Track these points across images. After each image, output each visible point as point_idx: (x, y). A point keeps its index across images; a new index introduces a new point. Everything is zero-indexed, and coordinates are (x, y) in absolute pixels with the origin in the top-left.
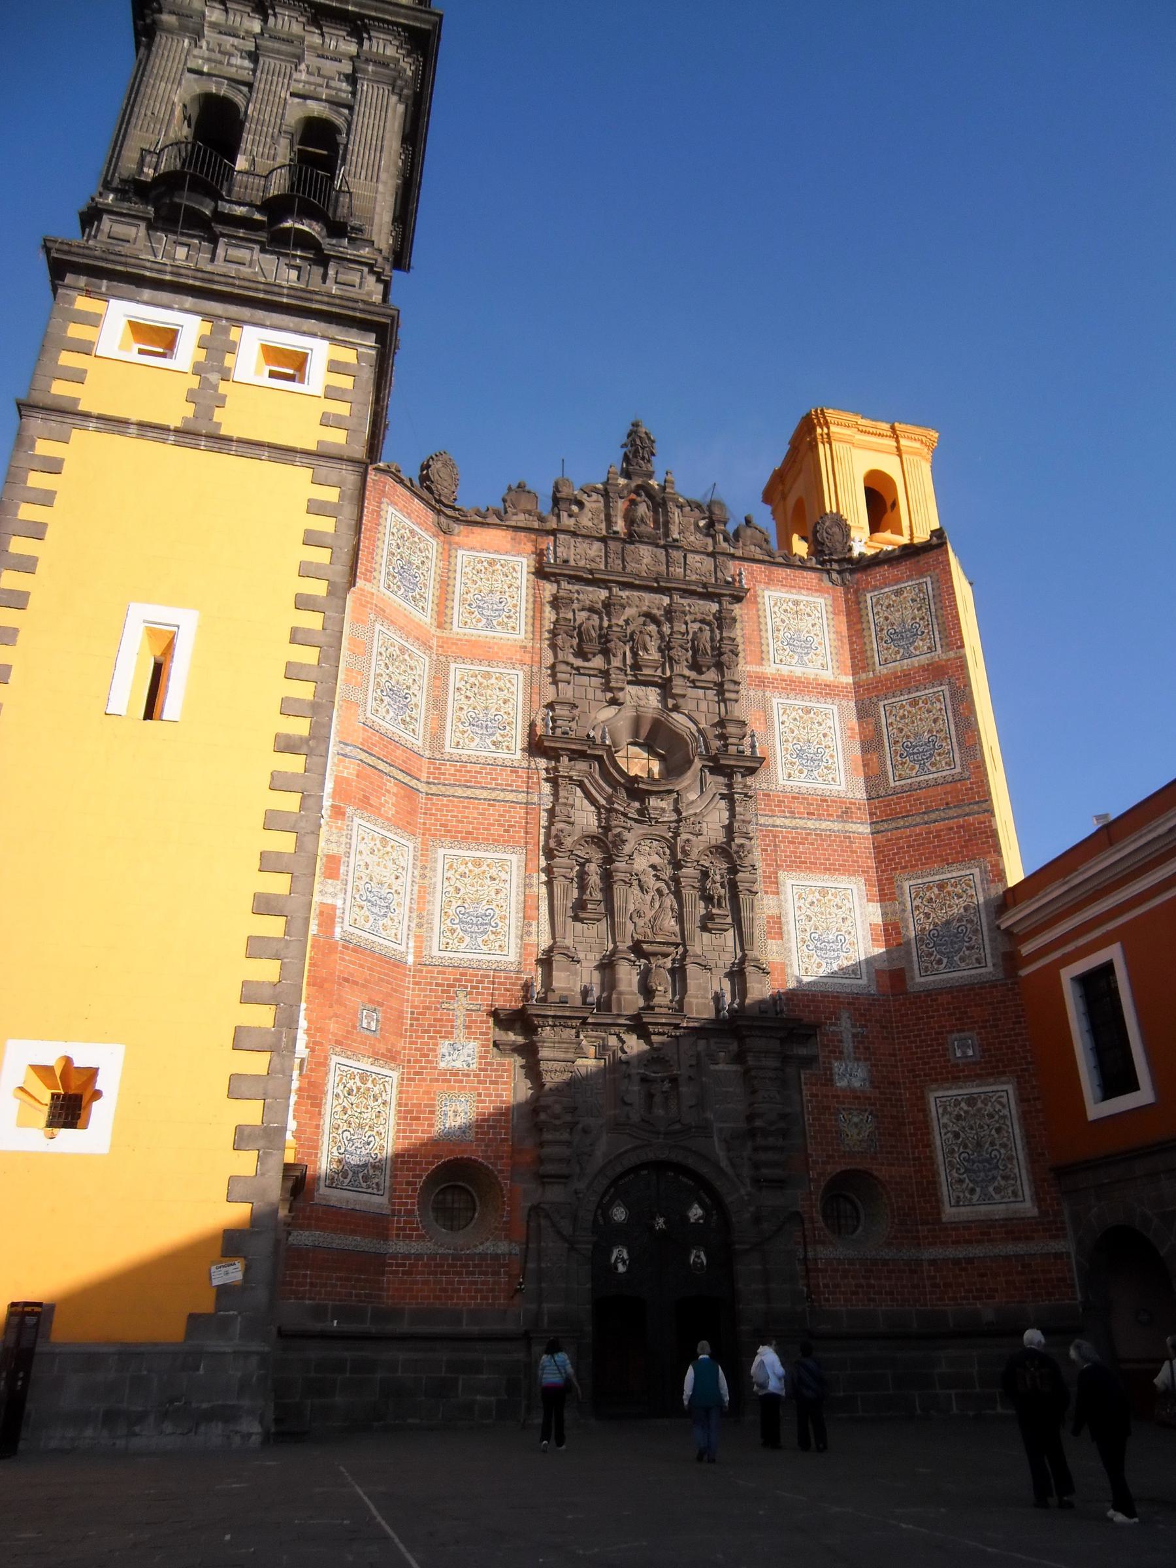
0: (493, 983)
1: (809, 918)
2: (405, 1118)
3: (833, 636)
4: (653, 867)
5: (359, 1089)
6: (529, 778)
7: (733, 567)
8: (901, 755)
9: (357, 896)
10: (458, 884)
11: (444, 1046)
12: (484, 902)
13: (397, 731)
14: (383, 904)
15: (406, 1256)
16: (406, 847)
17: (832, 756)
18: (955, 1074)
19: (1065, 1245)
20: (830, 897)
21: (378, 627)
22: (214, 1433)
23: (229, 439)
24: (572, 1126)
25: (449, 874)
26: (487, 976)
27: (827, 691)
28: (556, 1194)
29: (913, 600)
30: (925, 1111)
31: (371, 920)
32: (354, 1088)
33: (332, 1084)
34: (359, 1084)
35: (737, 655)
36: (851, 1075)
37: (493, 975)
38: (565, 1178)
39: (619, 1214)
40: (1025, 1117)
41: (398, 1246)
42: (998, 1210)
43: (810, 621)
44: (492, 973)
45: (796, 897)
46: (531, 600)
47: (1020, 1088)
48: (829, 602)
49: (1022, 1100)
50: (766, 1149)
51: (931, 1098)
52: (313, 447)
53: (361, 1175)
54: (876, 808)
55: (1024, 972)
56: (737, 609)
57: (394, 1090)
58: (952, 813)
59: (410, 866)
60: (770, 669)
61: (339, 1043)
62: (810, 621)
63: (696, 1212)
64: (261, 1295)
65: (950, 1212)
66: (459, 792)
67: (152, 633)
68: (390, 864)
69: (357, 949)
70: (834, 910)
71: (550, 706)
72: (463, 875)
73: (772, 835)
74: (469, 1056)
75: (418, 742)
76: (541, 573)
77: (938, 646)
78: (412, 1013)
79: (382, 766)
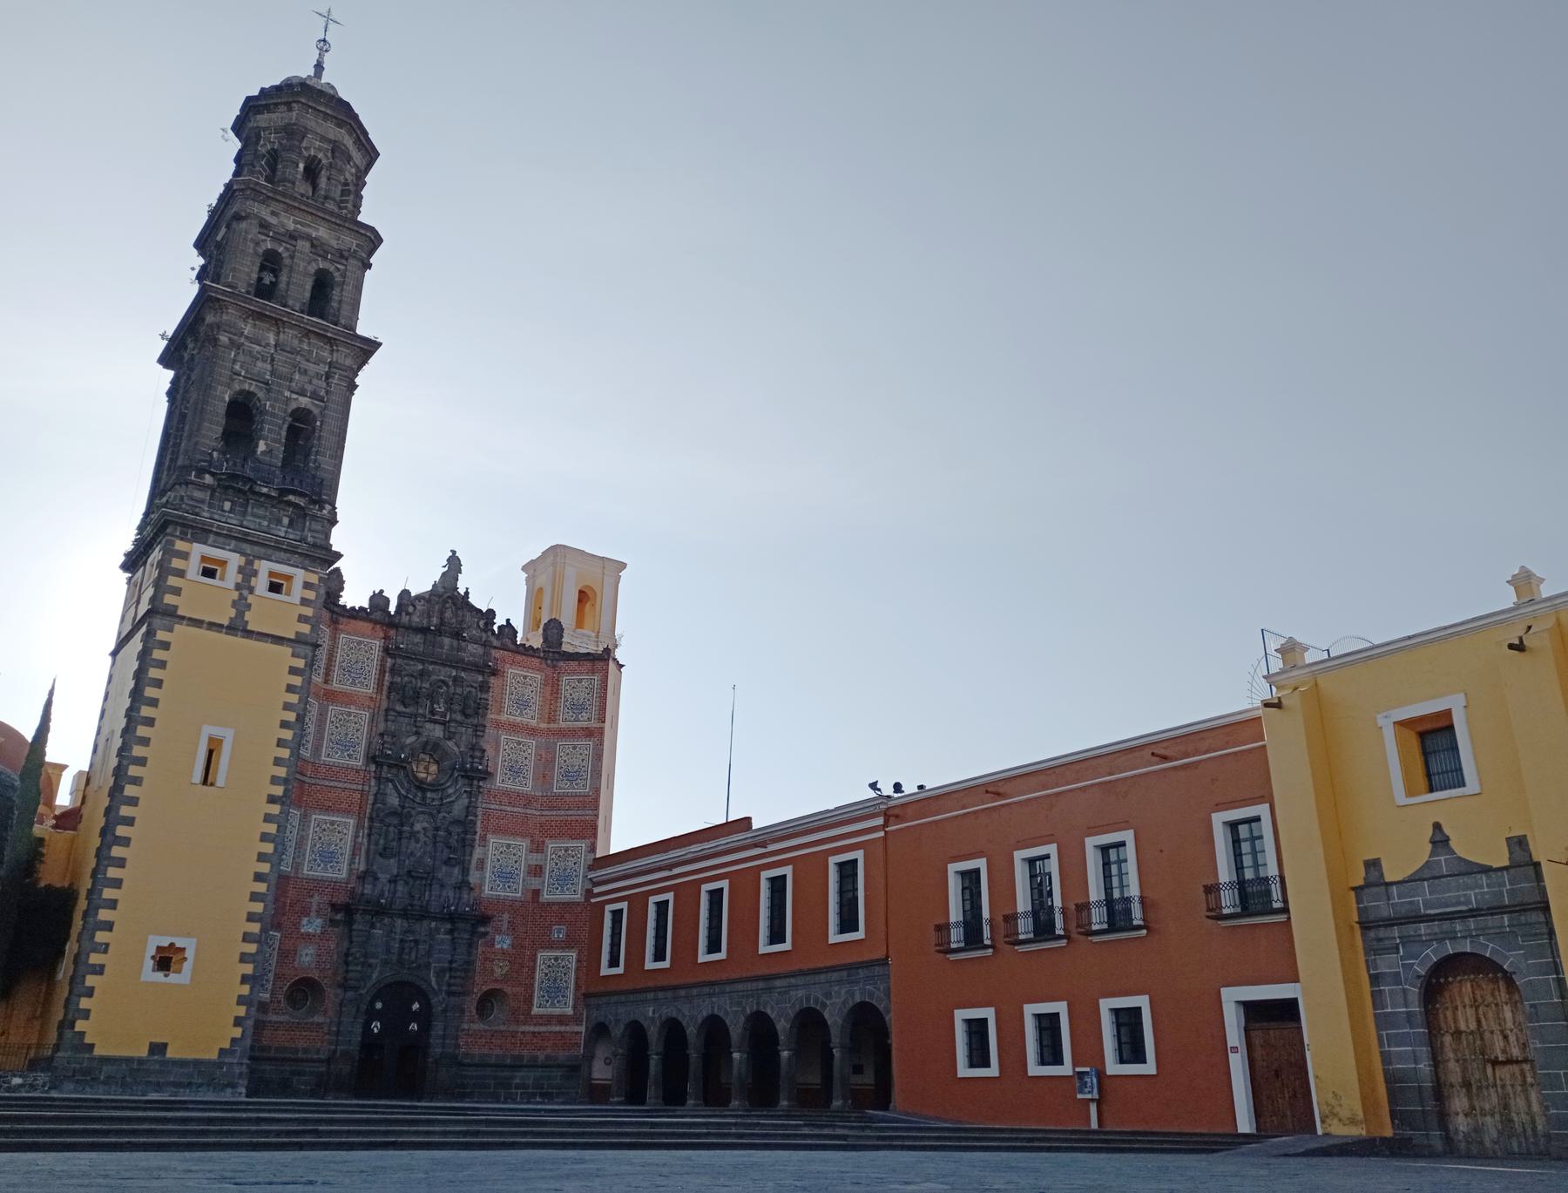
7: (495, 653)
11: (305, 921)
18: (551, 945)
19: (582, 1029)
23: (252, 632)
24: (363, 964)
27: (533, 732)
28: (350, 994)
30: (535, 961)
36: (503, 943)
37: (335, 885)
38: (356, 988)
39: (379, 1005)
42: (557, 1011)
49: (578, 961)
52: (292, 636)
56: (492, 680)
60: (504, 717)
63: (416, 1006)
64: (248, 1042)
65: (535, 1010)
71: (382, 735)
73: (487, 815)
76: (386, 650)
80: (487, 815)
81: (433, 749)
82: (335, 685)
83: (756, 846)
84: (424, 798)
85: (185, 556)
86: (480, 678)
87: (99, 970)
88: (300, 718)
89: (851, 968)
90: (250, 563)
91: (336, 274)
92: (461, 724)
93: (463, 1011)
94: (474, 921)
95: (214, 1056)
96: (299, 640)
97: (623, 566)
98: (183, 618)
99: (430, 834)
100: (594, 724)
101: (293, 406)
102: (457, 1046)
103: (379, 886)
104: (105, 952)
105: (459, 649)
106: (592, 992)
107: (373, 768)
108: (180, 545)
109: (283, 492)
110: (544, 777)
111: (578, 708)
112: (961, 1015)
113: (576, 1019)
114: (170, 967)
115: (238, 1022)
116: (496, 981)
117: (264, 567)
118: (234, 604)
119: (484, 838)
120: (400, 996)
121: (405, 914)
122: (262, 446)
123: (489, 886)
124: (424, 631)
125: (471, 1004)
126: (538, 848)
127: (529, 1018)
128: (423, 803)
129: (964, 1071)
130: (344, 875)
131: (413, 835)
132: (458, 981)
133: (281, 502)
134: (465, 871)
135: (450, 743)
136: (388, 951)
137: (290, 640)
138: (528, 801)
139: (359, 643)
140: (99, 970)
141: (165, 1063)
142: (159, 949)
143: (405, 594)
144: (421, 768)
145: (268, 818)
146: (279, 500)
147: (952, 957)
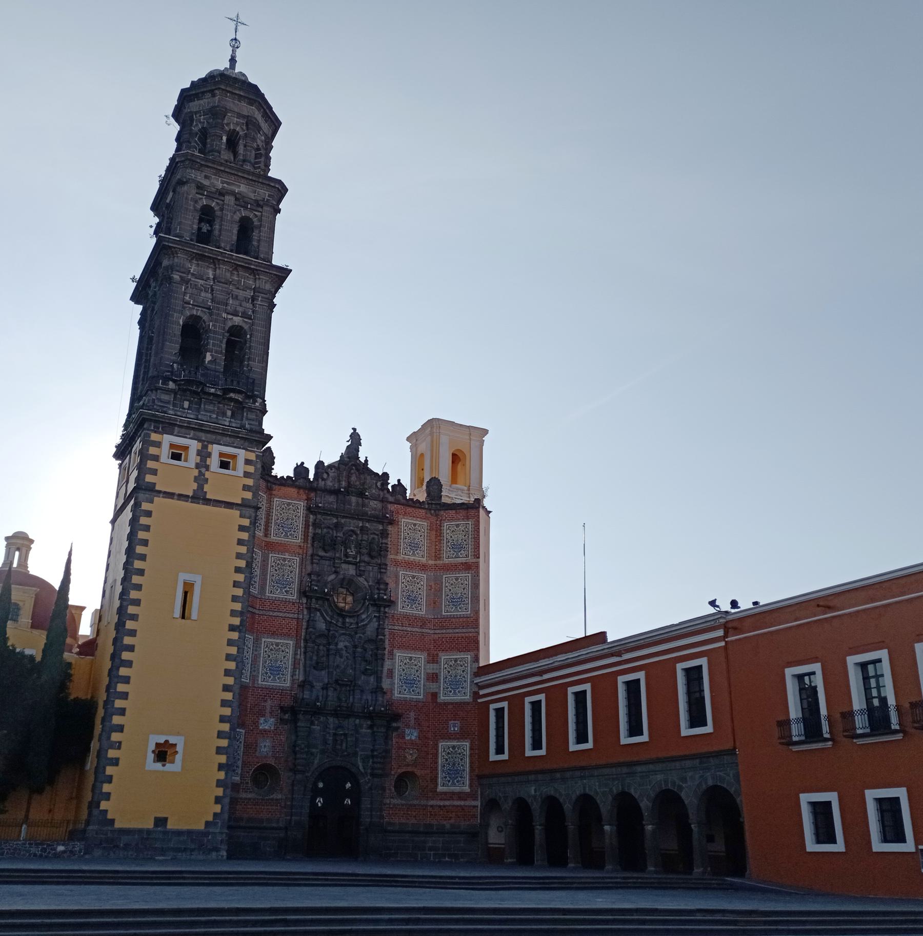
4: (345, 647)
7: (391, 507)
11: (262, 720)
15: (246, 799)
18: (449, 737)
19: (478, 803)
22: (214, 855)
23: (210, 500)
27: (423, 568)
28: (299, 777)
36: (412, 735)
39: (321, 785)
40: (471, 755)
41: (243, 795)
42: (457, 789)
47: (471, 745)
49: (471, 749)
50: (377, 763)
51: (440, 745)
52: (239, 502)
55: (479, 701)
56: (390, 528)
58: (464, 630)
60: (400, 557)
63: (348, 785)
64: (226, 816)
65: (440, 789)
66: (271, 614)
67: (185, 584)
71: (309, 575)
73: (392, 634)
76: (309, 509)
80: (392, 634)
81: (348, 584)
82: (273, 538)
83: (612, 655)
84: (344, 623)
85: (158, 445)
86: (381, 527)
87: (115, 762)
88: (249, 565)
89: (703, 757)
90: (205, 447)
91: (255, 219)
92: (368, 563)
93: (384, 789)
94: (389, 718)
95: (201, 827)
96: (244, 505)
97: (485, 432)
98: (160, 492)
99: (351, 651)
100: (470, 559)
101: (230, 324)
102: (382, 817)
103: (315, 692)
104: (119, 748)
105: (363, 505)
106: (484, 774)
108: (154, 437)
109: (226, 391)
110: (434, 603)
111: (457, 547)
112: (805, 799)
113: (472, 796)
114: (167, 760)
115: (218, 800)
116: (408, 765)
117: (216, 450)
118: (196, 479)
119: (391, 653)
120: (336, 777)
121: (336, 714)
122: (208, 357)
123: (398, 692)
124: (335, 492)
125: (390, 783)
126: (433, 659)
127: (435, 794)
128: (344, 627)
129: (811, 846)
131: (338, 652)
132: (379, 765)
133: (224, 399)
134: (379, 679)
135: (361, 579)
136: (325, 742)
137: (237, 504)
138: (423, 622)
139: (289, 504)
140: (115, 762)
141: (166, 833)
142: (157, 745)
143: (320, 464)
144: (340, 600)
145: (230, 643)
146: (223, 398)
147: (795, 748)
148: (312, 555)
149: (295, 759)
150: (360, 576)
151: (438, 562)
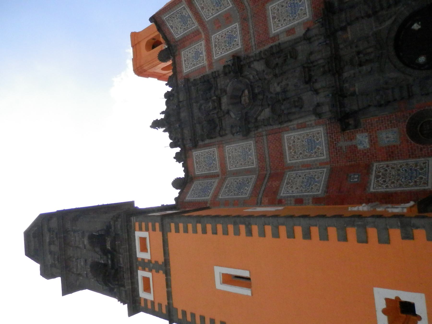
0: (332, 134)
1: (285, 20)
2: (393, 157)
3: (192, 45)
4: (278, 84)
5: (383, 178)
6: (258, 137)
8: (221, 6)
9: (308, 190)
10: (299, 154)
11: (360, 147)
12: (303, 143)
13: (251, 185)
14: (310, 180)
16: (288, 174)
17: (228, 32)
20: (275, 15)
21: (220, 197)
23: (165, 260)
25: (296, 157)
26: (330, 136)
27: (208, 41)
29: (172, 21)
31: (316, 183)
32: (382, 180)
33: (382, 190)
34: (381, 178)
35: (204, 76)
39: (422, 59)
43: (189, 54)
44: (329, 135)
45: (278, 28)
46: (204, 148)
48: (182, 50)
53: (420, 172)
54: (241, 9)
57: (381, 163)
59: (295, 172)
60: (206, 63)
61: (365, 189)
62: (189, 54)
63: (416, 26)
66: (267, 159)
68: (295, 180)
69: (328, 187)
70: (280, 11)
71: (233, 134)
72: (295, 152)
74: (362, 137)
75: (254, 177)
77: (182, 6)
78: (349, 162)
79: (263, 188)
82: (218, 170)
107: (252, 134)
117: (140, 255)
118: (157, 272)
119: (274, 38)
130: (321, 129)
131: (284, 91)
138: (244, 20)
139: (197, 163)
143: (172, 146)
148: (221, 136)
149: (395, 100)
150: (225, 91)
151: (201, 30)
